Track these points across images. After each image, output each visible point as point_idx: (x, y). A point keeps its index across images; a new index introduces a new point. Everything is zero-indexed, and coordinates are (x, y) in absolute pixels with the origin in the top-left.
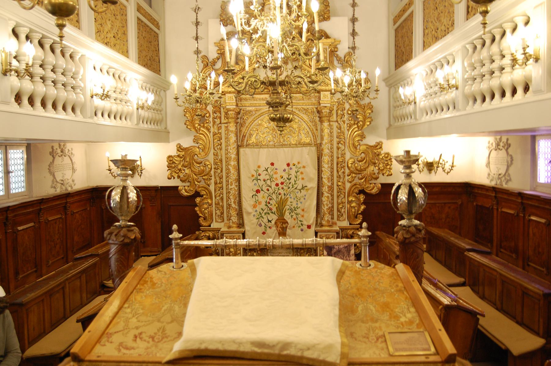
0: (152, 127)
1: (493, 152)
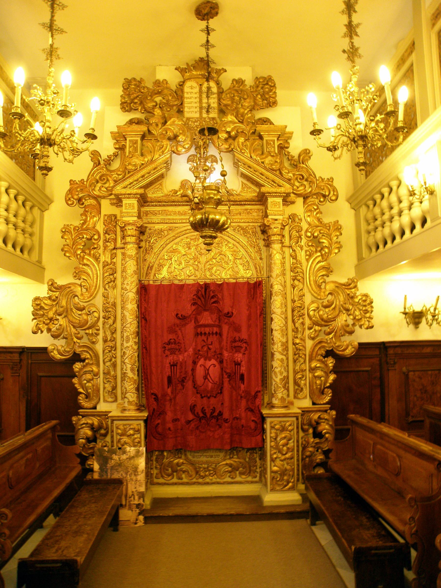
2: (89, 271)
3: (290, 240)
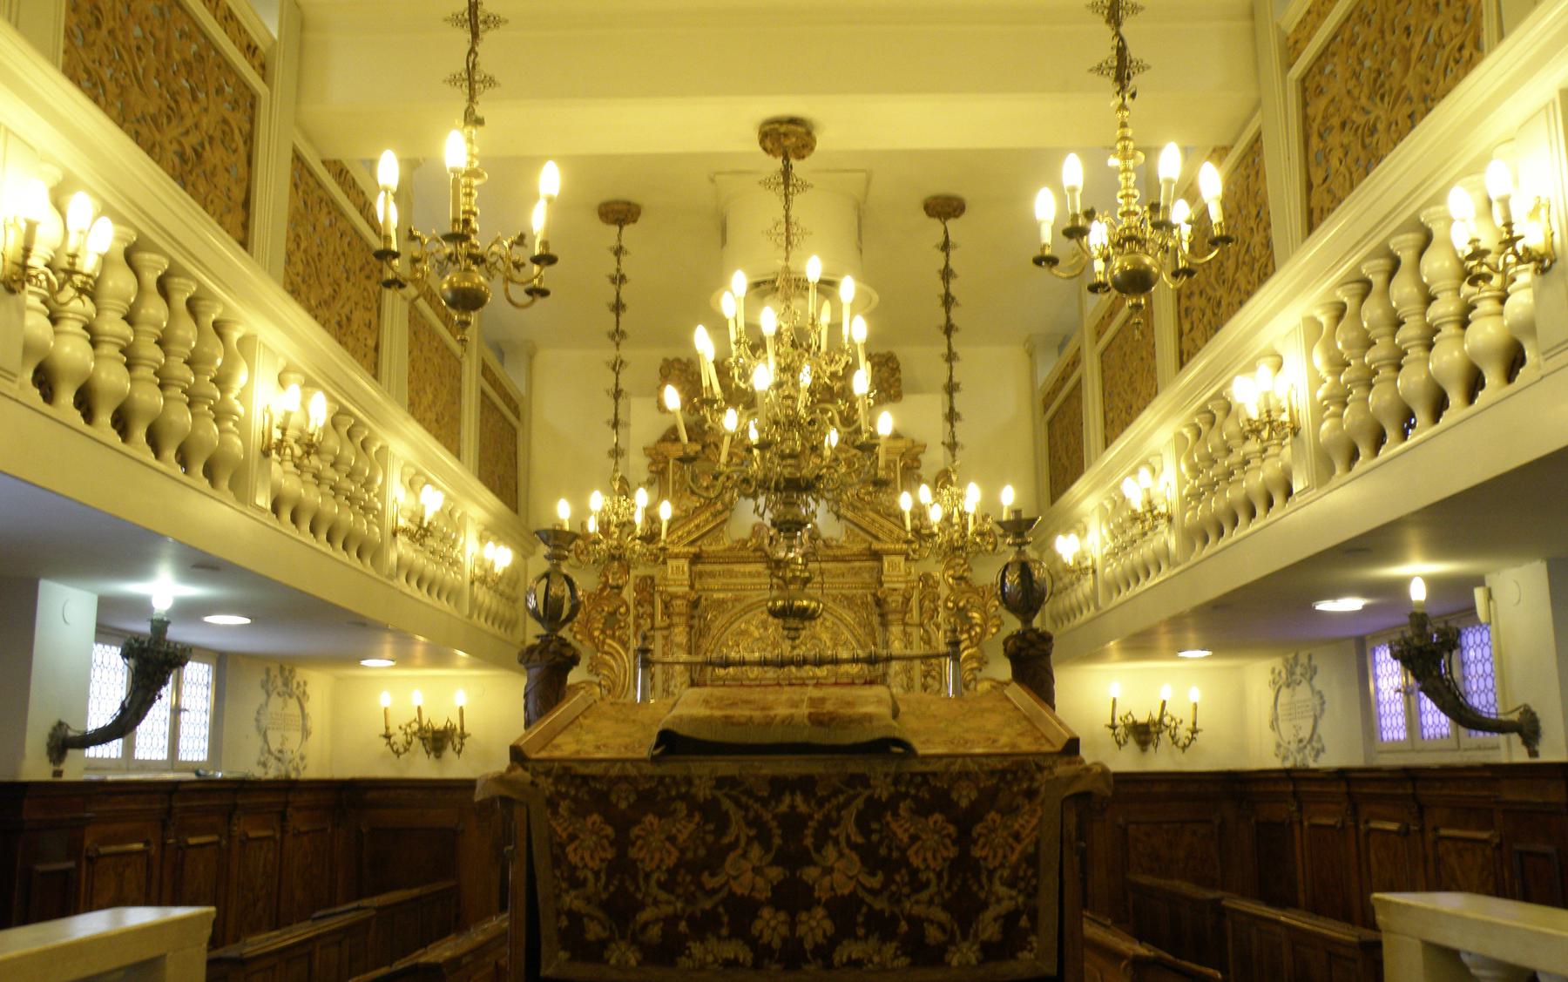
0: (495, 630)
1: (1284, 691)
2: (612, 662)
3: (921, 614)
